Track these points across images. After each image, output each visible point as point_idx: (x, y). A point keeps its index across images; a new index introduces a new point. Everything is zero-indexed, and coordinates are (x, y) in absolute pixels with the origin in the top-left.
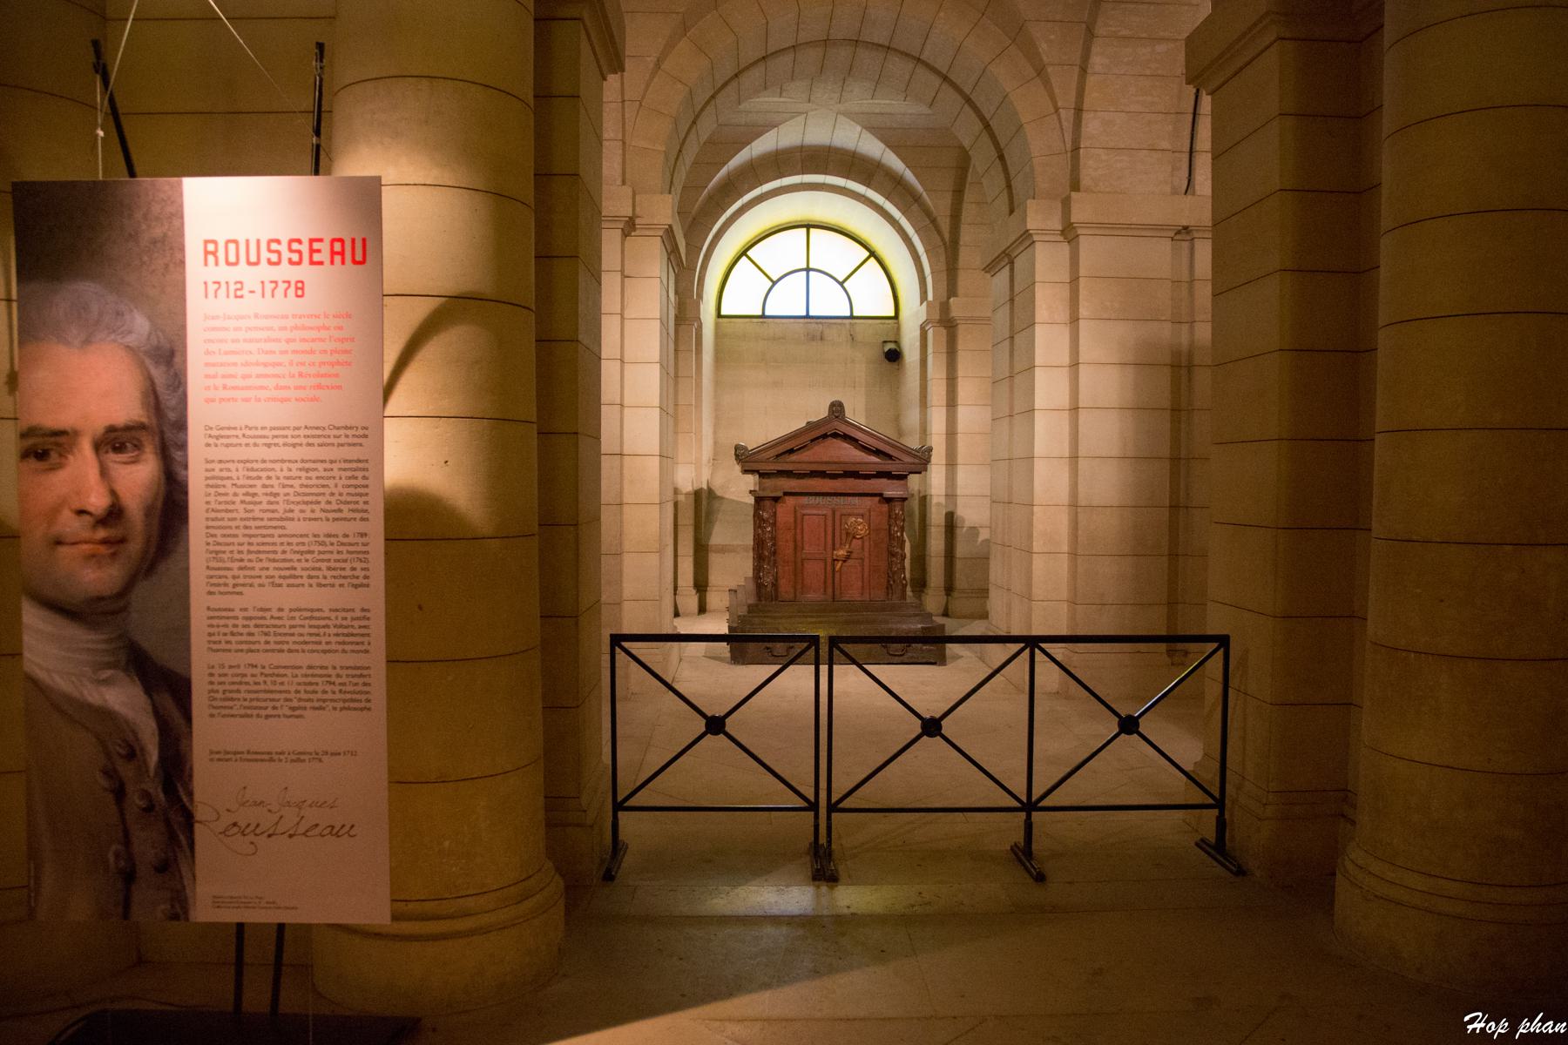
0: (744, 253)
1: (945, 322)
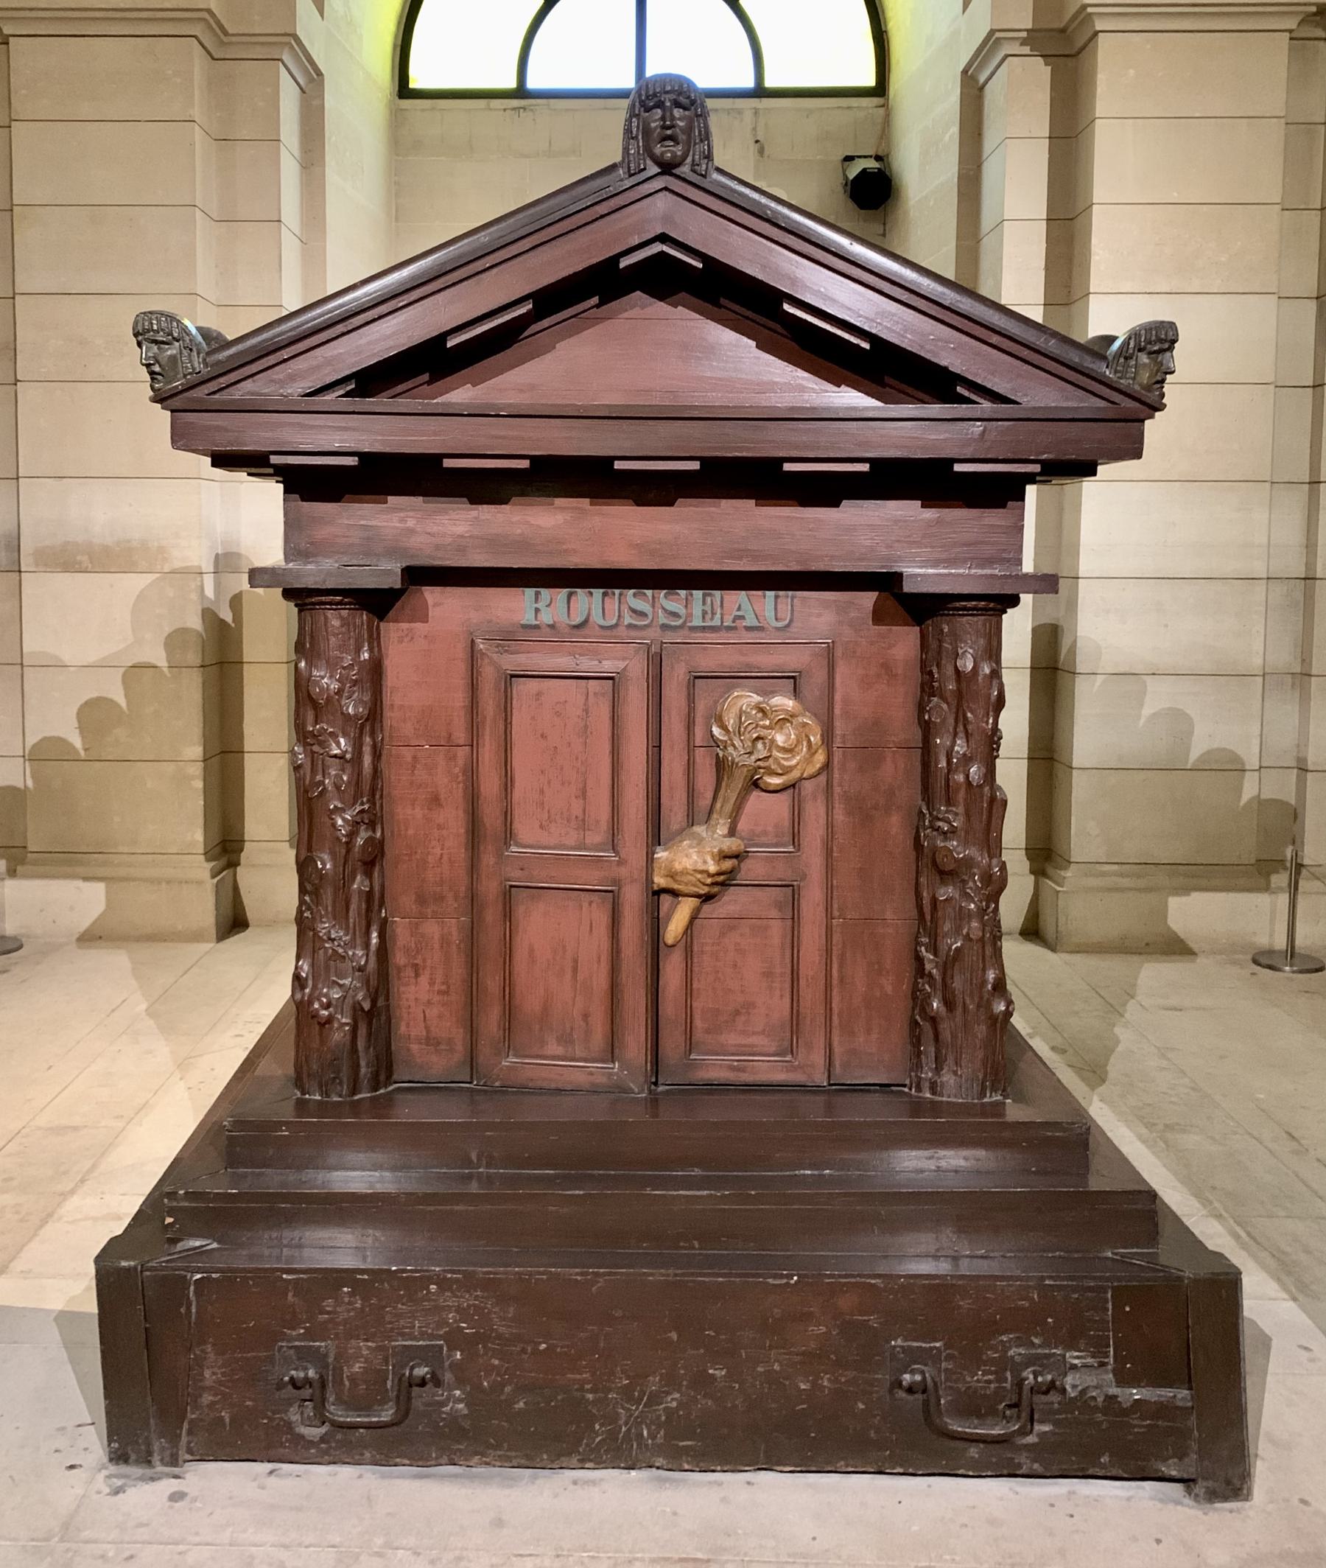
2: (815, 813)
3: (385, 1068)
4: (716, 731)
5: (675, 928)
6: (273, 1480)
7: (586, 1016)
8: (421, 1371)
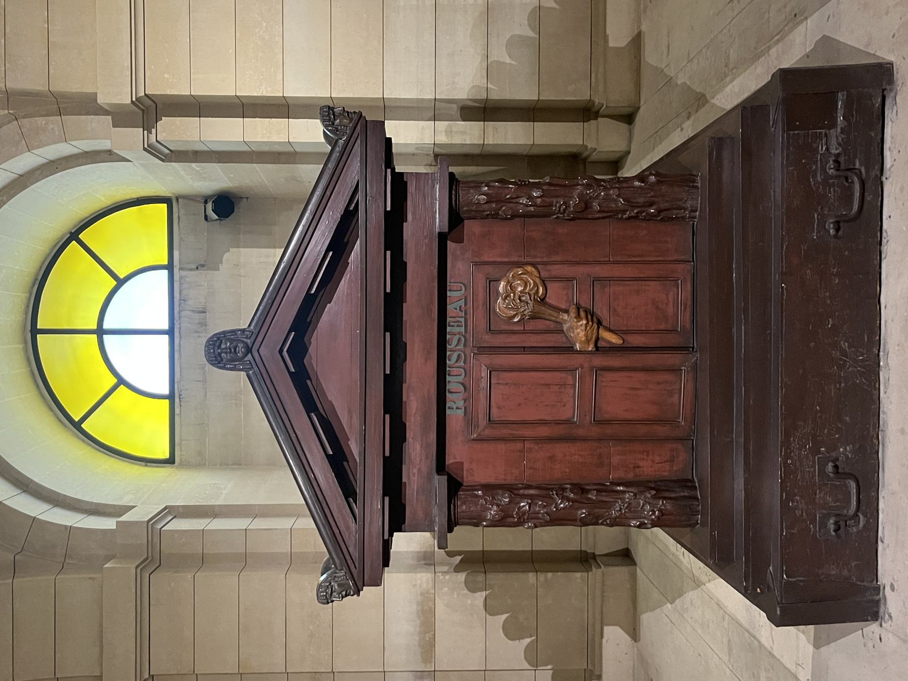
0: (77, 426)
2: (557, 270)
3: (686, 483)
4: (516, 320)
5: (614, 339)
6: (885, 541)
7: (659, 383)
8: (830, 467)
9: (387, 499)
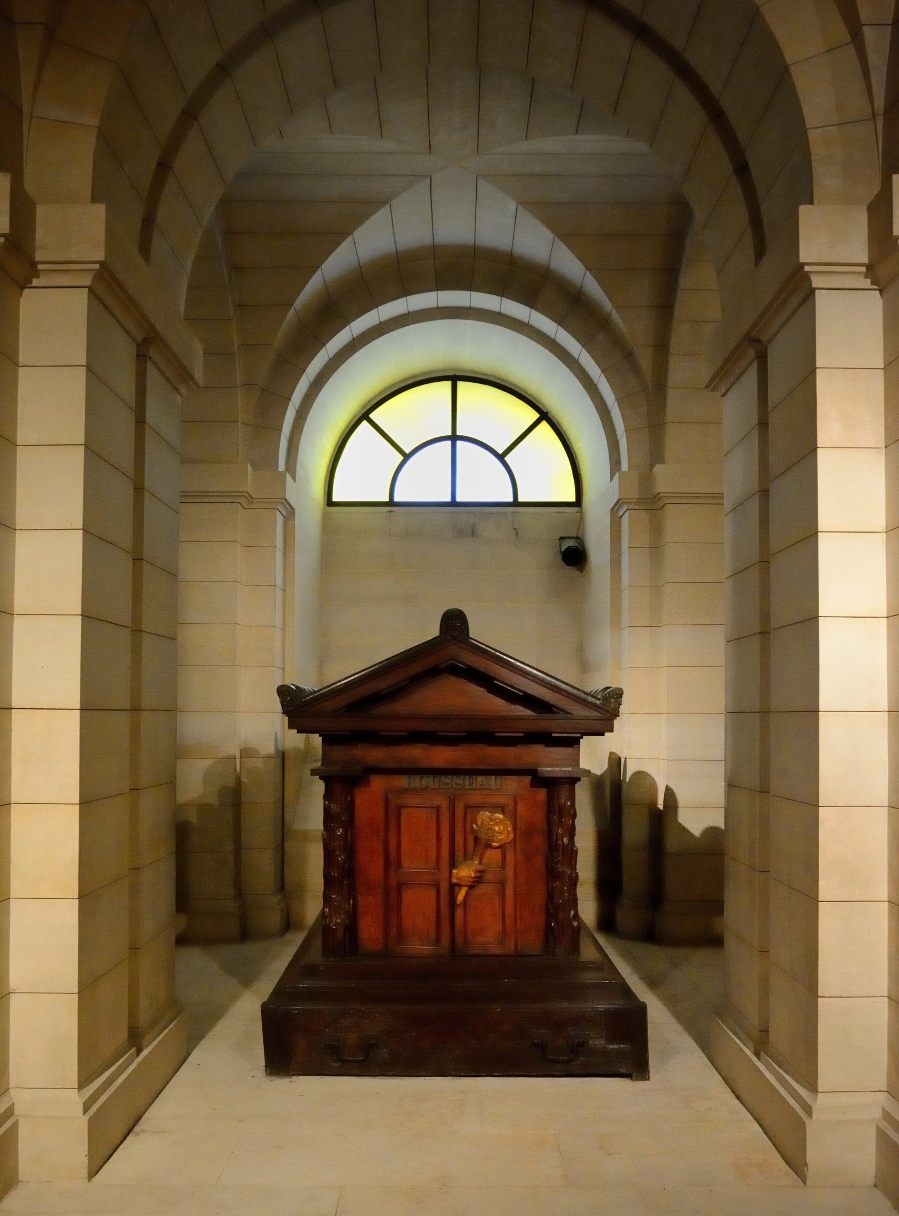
0: (365, 416)
1: (646, 502)
9: (347, 733)
